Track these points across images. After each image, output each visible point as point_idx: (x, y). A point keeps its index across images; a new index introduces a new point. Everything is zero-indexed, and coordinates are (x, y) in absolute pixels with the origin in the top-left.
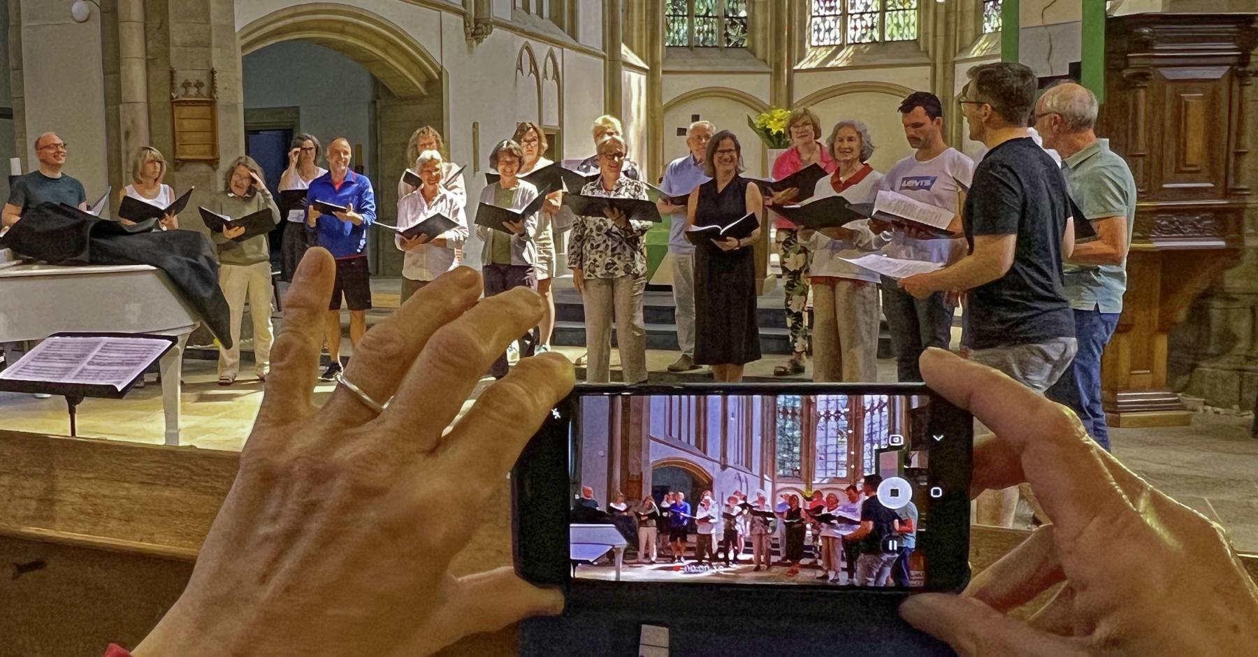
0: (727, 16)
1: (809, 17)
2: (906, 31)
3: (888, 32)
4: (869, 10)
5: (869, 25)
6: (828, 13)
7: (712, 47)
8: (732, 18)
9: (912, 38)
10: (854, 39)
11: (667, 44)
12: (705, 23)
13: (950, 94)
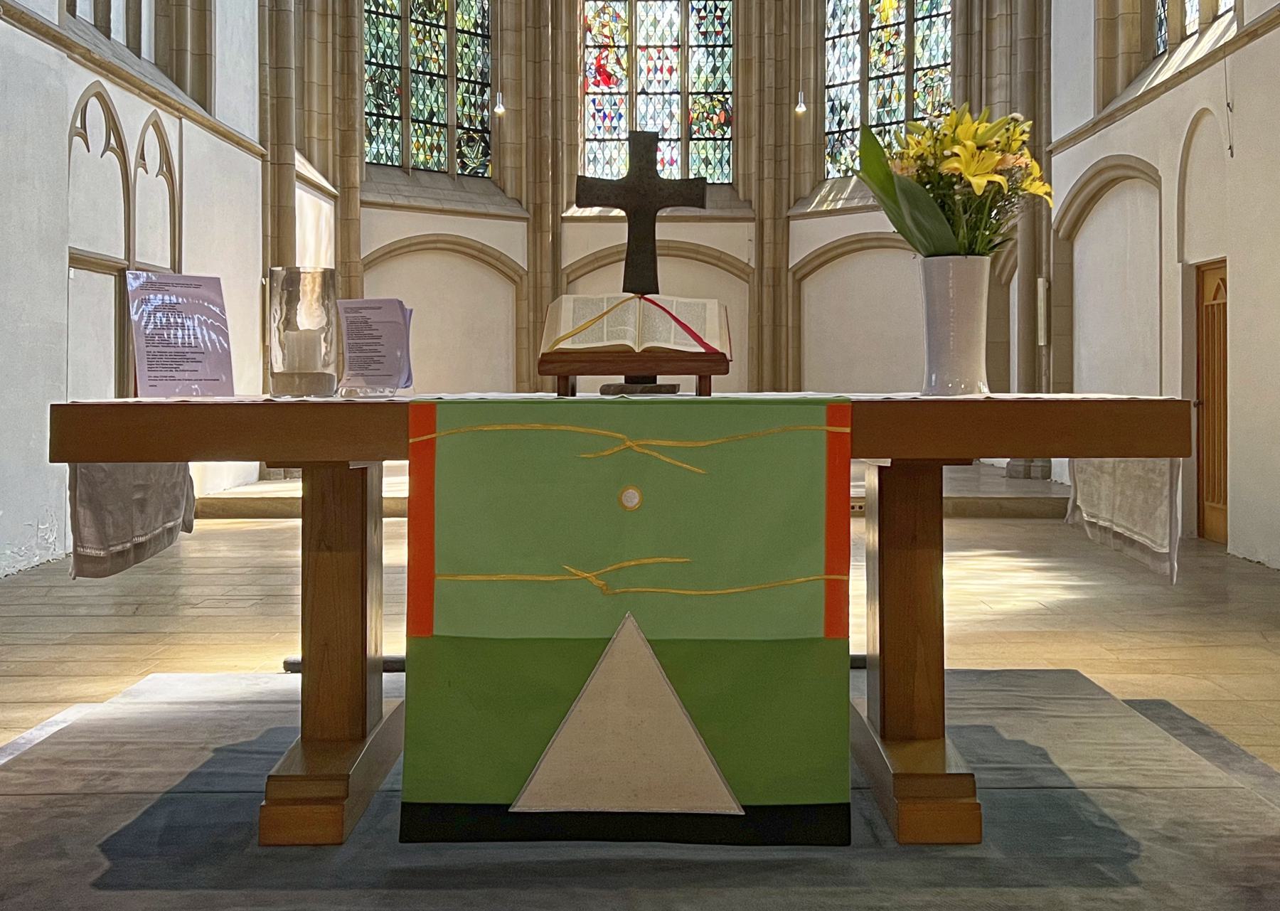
1: (580, 140)
6: (608, 136)
7: (438, 172)
8: (468, 130)
9: (726, 181)
11: (367, 160)
12: (427, 133)
13: (784, 265)
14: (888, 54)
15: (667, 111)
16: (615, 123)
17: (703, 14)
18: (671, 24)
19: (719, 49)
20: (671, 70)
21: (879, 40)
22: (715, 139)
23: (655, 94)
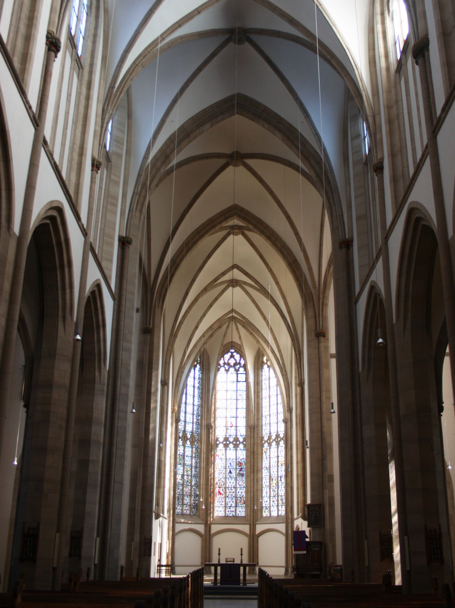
0: (192, 505)
2: (242, 513)
3: (237, 513)
4: (232, 506)
5: (232, 511)
6: (220, 506)
9: (244, 516)
10: (228, 514)
14: (274, 492)
15: (232, 501)
16: (222, 503)
17: (239, 481)
18: (233, 483)
19: (242, 488)
20: (233, 492)
21: (273, 489)
22: (242, 507)
23: (230, 497)
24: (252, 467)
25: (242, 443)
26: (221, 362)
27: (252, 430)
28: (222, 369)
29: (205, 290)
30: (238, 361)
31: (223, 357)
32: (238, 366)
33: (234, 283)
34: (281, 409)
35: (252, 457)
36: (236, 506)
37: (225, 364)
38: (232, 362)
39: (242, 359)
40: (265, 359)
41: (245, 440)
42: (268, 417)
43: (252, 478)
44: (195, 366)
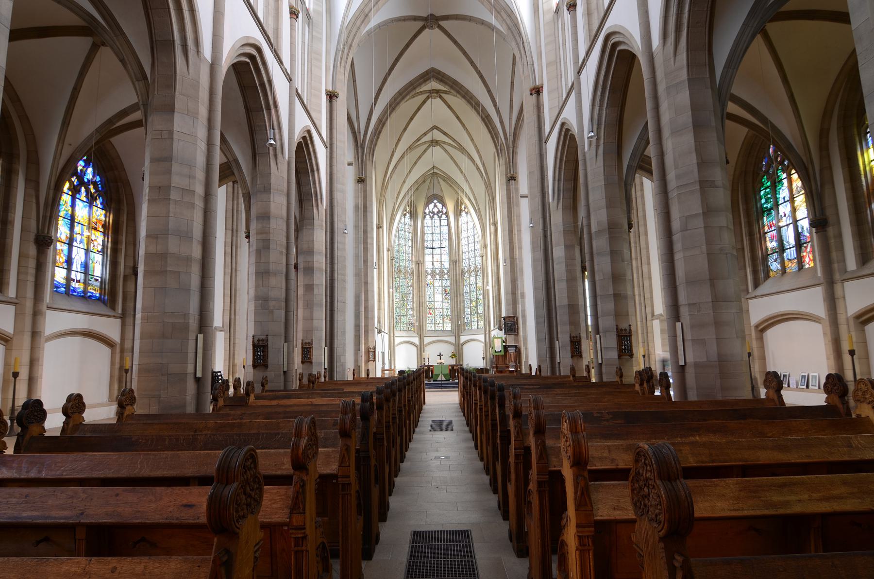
24: (455, 292)
25: (447, 273)
26: (427, 211)
27: (454, 263)
28: (428, 217)
29: (410, 148)
30: (440, 210)
31: (428, 206)
32: (441, 213)
33: (434, 143)
34: (478, 246)
35: (455, 284)
36: (443, 323)
37: (429, 212)
38: (436, 210)
39: (444, 208)
40: (463, 206)
41: (448, 271)
42: (467, 253)
43: (456, 301)
44: (405, 215)
